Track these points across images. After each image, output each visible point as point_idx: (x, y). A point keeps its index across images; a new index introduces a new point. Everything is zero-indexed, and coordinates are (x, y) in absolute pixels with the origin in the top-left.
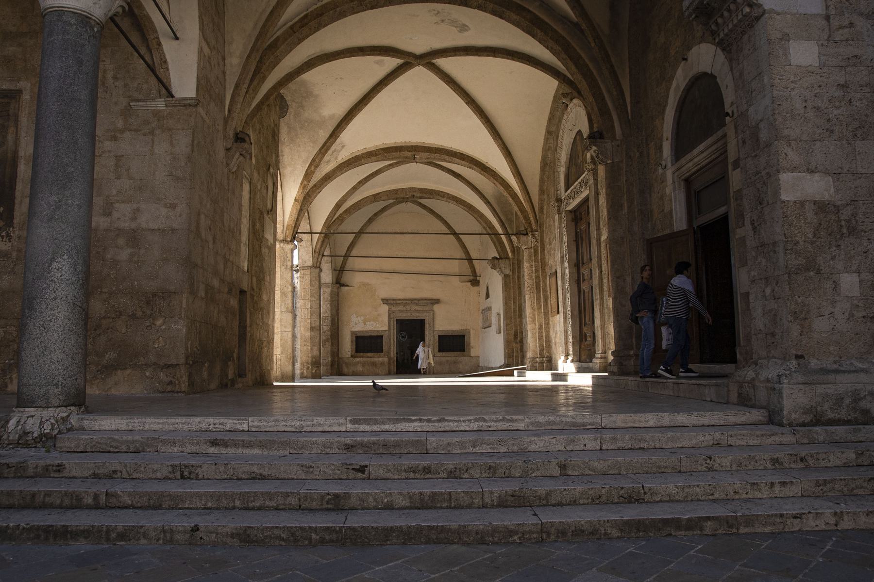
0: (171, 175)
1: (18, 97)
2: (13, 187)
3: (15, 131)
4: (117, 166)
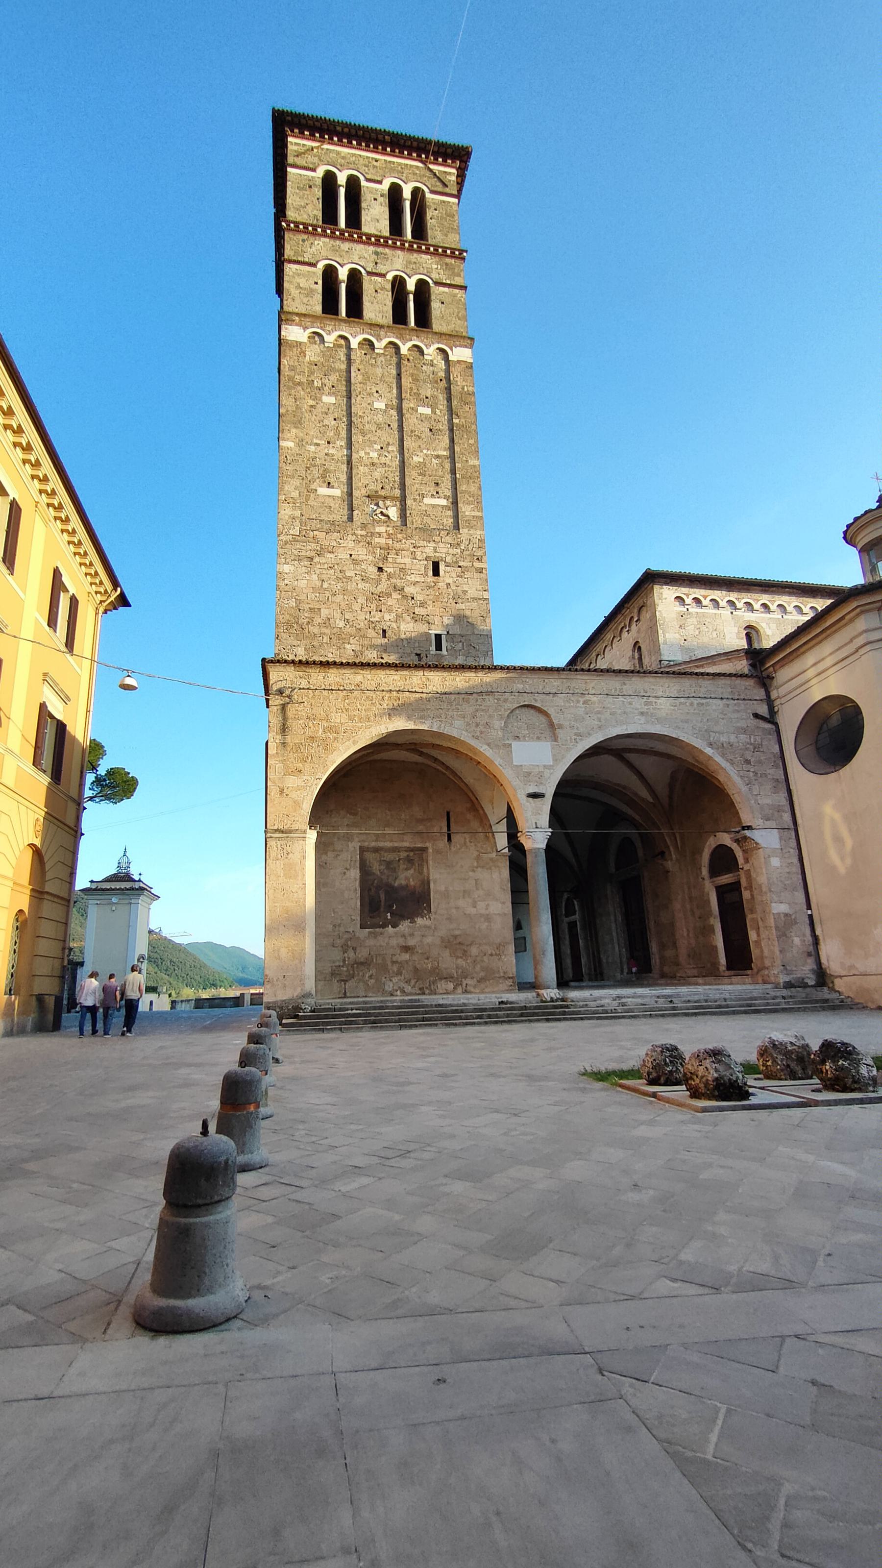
0: (501, 888)
2: (430, 895)
4: (476, 883)
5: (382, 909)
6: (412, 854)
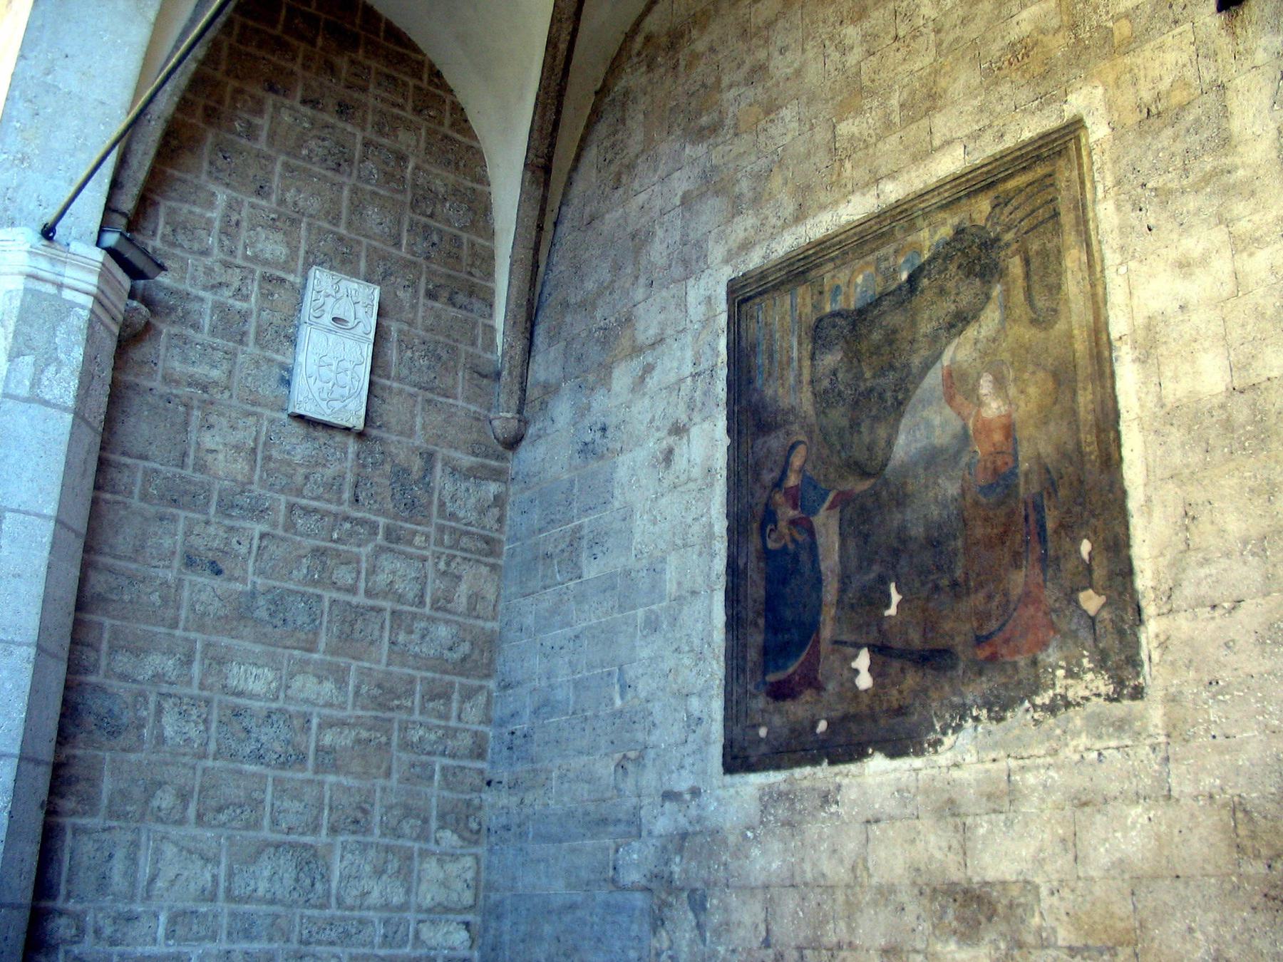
1: (1072, 145)
2: (1111, 461)
3: (1084, 258)
5: (826, 632)
6: (983, 205)
